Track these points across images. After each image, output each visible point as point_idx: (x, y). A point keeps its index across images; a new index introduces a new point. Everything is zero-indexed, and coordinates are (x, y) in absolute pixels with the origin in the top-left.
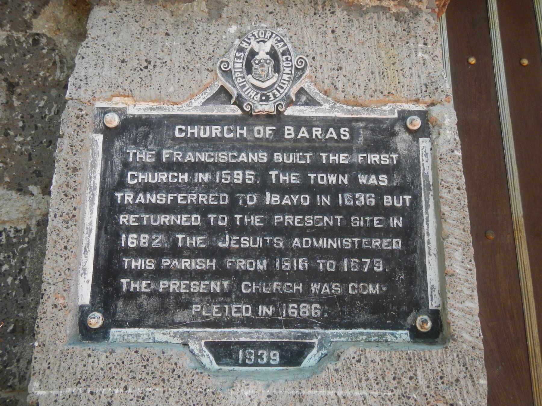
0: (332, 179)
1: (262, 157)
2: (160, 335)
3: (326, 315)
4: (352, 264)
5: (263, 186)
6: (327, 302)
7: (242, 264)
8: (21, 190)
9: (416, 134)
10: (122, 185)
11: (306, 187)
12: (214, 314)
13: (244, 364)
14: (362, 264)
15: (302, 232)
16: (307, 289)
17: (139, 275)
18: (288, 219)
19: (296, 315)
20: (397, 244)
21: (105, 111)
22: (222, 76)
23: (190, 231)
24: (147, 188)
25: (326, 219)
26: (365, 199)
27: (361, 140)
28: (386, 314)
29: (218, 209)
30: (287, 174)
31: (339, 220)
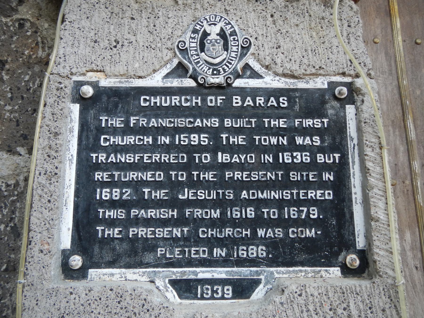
0: (274, 140)
1: (214, 122)
2: (132, 274)
3: (270, 256)
4: (292, 212)
5: (216, 147)
6: (272, 244)
7: (198, 213)
8: (11, 151)
9: (343, 102)
10: (96, 147)
11: (251, 147)
12: (176, 256)
13: (202, 298)
14: (300, 212)
15: (248, 185)
16: (254, 233)
17: (112, 223)
18: (238, 175)
19: (245, 256)
20: (329, 195)
21: (81, 84)
22: (180, 54)
23: (156, 185)
24: (117, 149)
25: (269, 174)
26: (301, 157)
27: (297, 108)
28: (321, 253)
29: (180, 167)
30: (236, 137)
31: (280, 175)
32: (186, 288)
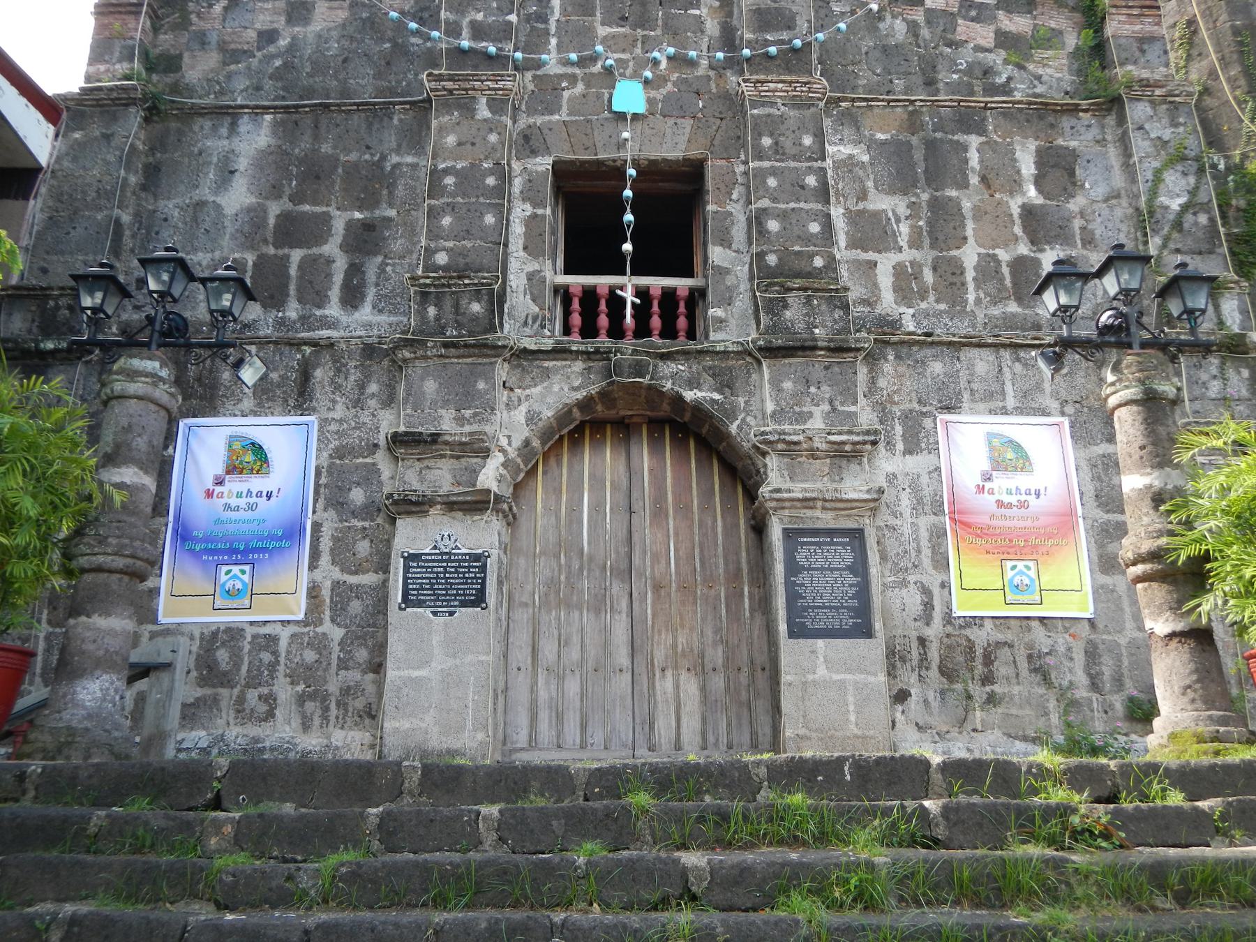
11: (456, 572)
32: (435, 614)
